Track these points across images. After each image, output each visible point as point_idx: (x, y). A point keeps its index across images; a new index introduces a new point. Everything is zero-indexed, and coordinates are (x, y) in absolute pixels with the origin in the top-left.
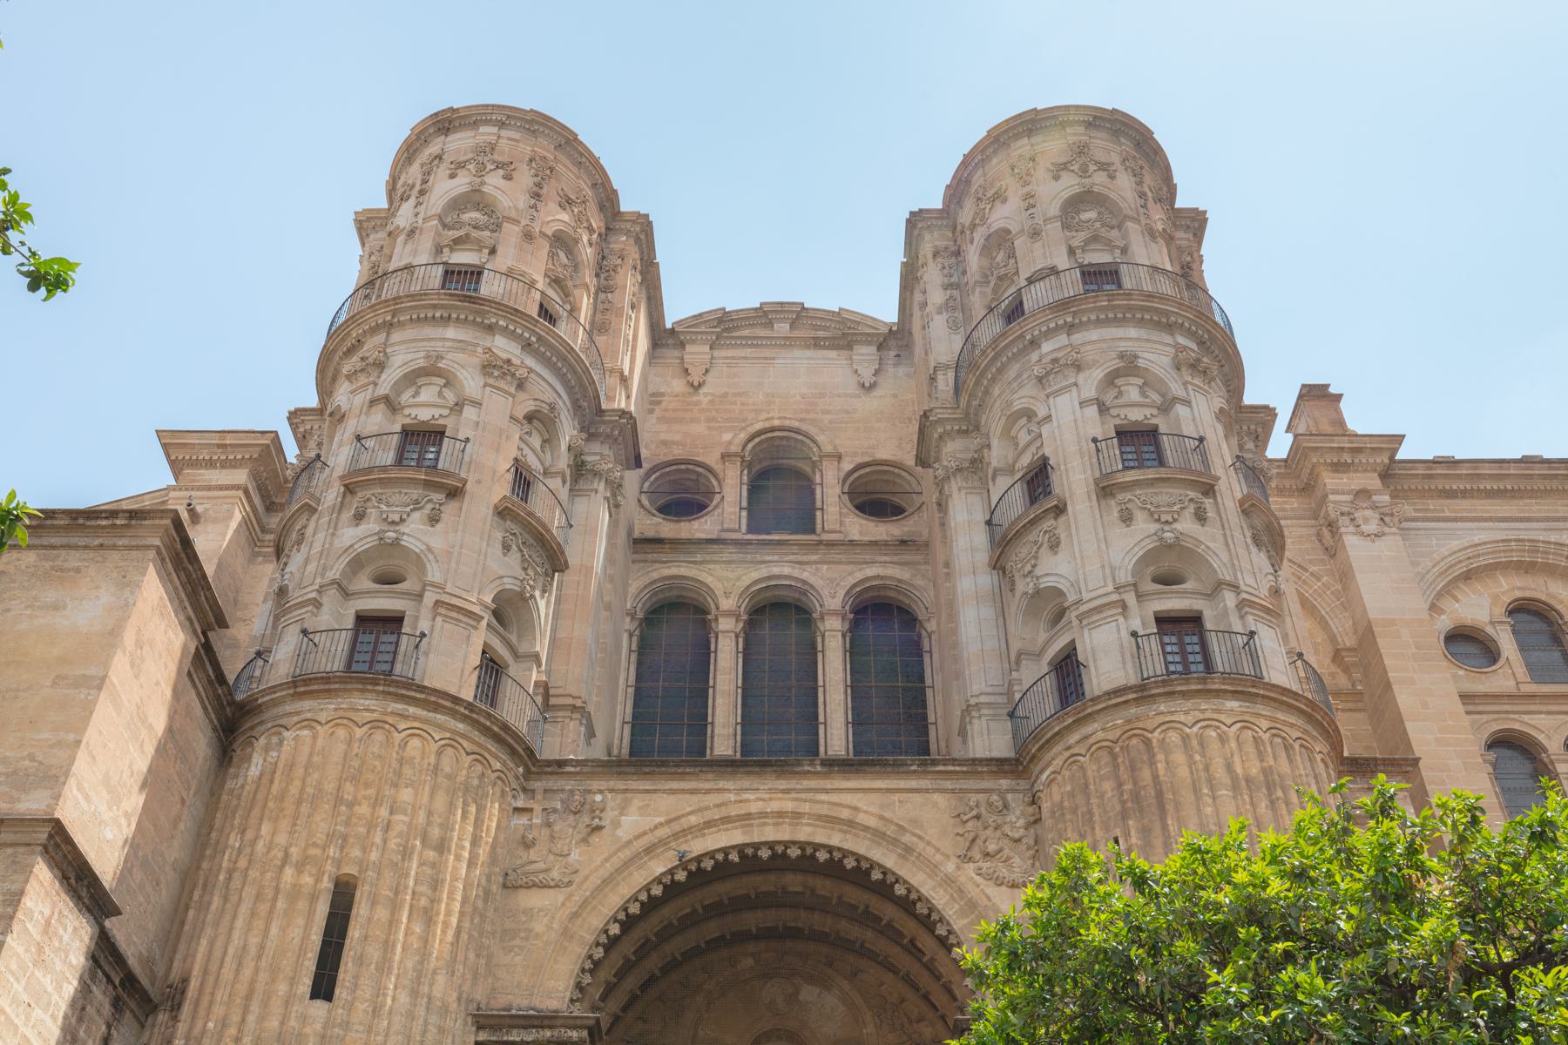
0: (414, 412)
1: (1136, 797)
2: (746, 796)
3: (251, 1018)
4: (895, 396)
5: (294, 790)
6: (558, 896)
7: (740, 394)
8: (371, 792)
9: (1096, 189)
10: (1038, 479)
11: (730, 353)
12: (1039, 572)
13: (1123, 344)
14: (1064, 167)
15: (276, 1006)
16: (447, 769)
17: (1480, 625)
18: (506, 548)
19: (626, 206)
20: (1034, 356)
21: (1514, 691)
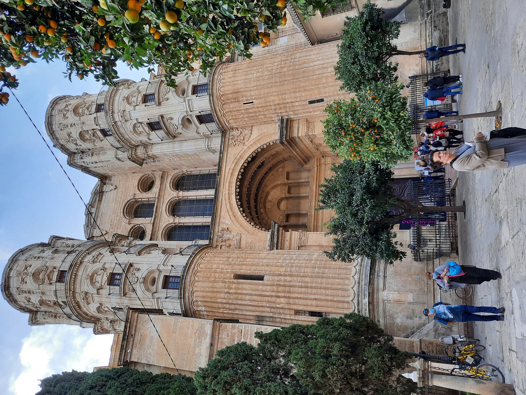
1: (235, 98)
2: (224, 194)
3: (267, 294)
5: (209, 294)
6: (243, 236)
7: (111, 221)
8: (213, 274)
9: (73, 108)
10: (153, 126)
12: (177, 124)
14: (64, 115)
16: (209, 258)
18: (150, 253)
19: (46, 241)
20: (119, 123)
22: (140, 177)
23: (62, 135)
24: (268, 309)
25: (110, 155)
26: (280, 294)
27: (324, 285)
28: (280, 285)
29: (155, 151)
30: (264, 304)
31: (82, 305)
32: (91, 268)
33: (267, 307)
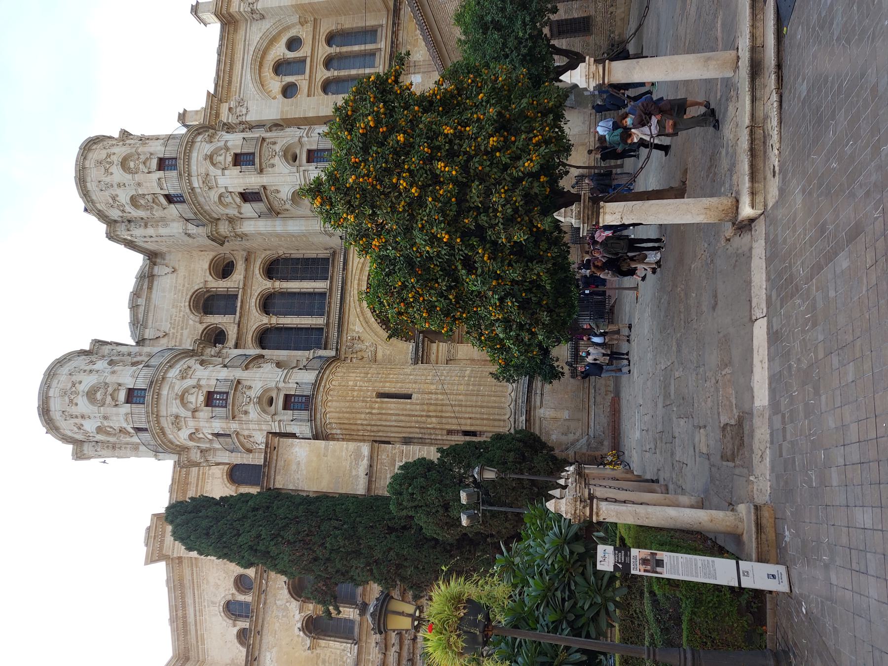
0: (199, 402)
3: (416, 413)
4: (179, 261)
5: (347, 415)
6: (379, 347)
7: (171, 318)
10: (247, 197)
11: (150, 322)
12: (285, 199)
13: (199, 158)
14: (107, 170)
15: (414, 407)
17: (282, 86)
18: (260, 367)
19: (87, 348)
20: (198, 190)
21: (307, 82)
22: (211, 257)
23: (101, 198)
24: (418, 430)
25: (176, 228)
26: (431, 414)
27: (479, 404)
28: (431, 404)
29: (248, 227)
30: (413, 424)
31: (168, 431)
32: (180, 386)
33: (416, 427)
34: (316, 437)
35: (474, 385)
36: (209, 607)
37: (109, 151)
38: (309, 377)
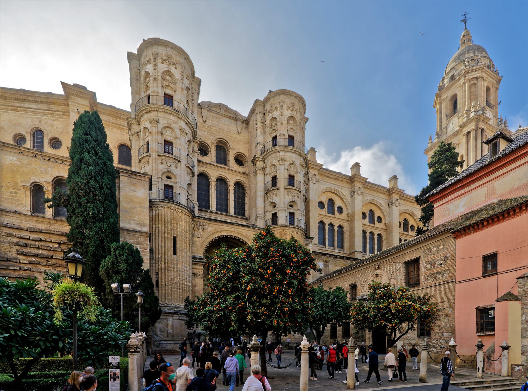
0: (167, 137)
30: (160, 255)
31: (149, 115)
34: (150, 201)
35: (182, 287)
36: (38, 118)
37: (298, 111)
38: (183, 201)
